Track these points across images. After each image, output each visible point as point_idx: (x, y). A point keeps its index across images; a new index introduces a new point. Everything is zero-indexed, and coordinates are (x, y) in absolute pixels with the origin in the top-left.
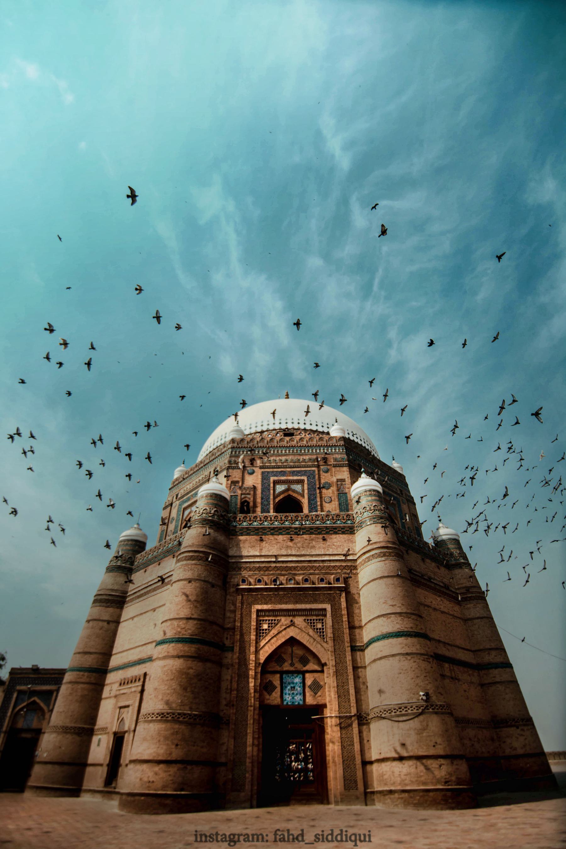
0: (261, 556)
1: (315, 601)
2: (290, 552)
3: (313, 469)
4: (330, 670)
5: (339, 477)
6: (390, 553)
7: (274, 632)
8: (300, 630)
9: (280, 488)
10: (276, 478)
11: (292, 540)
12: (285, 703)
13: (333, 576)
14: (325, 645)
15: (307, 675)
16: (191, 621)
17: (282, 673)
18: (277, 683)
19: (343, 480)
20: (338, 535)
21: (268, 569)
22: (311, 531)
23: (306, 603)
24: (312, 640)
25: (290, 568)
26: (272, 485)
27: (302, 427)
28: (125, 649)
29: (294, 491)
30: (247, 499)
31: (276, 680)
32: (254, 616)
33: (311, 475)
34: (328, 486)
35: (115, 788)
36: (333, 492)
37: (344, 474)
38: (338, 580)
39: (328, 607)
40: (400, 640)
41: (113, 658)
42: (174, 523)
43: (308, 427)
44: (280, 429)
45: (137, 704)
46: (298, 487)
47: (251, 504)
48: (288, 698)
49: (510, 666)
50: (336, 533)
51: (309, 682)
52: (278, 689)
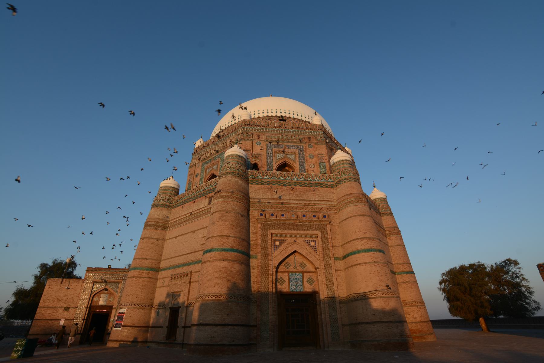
0: (272, 199)
1: (310, 229)
2: (291, 197)
3: (302, 145)
4: (321, 272)
5: (320, 152)
6: (361, 201)
7: (283, 247)
8: (300, 245)
9: (280, 156)
10: (276, 149)
11: (292, 190)
12: (291, 291)
13: (321, 214)
14: (317, 256)
15: (305, 274)
16: (230, 238)
17: (289, 273)
18: (286, 278)
19: (322, 154)
20: (323, 188)
21: (277, 207)
22: (305, 185)
23: (305, 230)
24: (309, 253)
25: (293, 208)
26: (274, 154)
27: (292, 116)
28: (171, 256)
29: (289, 158)
30: (257, 162)
31: (285, 277)
32: (270, 237)
33: (301, 149)
34: (312, 156)
35: (175, 340)
36: (316, 161)
37: (323, 149)
38: (325, 216)
39: (319, 233)
40: (370, 254)
41: (162, 263)
42: (199, 177)
43: (296, 117)
44: (276, 116)
45: (187, 290)
46: (292, 157)
47: (259, 166)
48: (293, 289)
49: (413, 273)
50: (322, 187)
51: (306, 279)
52: (287, 282)
